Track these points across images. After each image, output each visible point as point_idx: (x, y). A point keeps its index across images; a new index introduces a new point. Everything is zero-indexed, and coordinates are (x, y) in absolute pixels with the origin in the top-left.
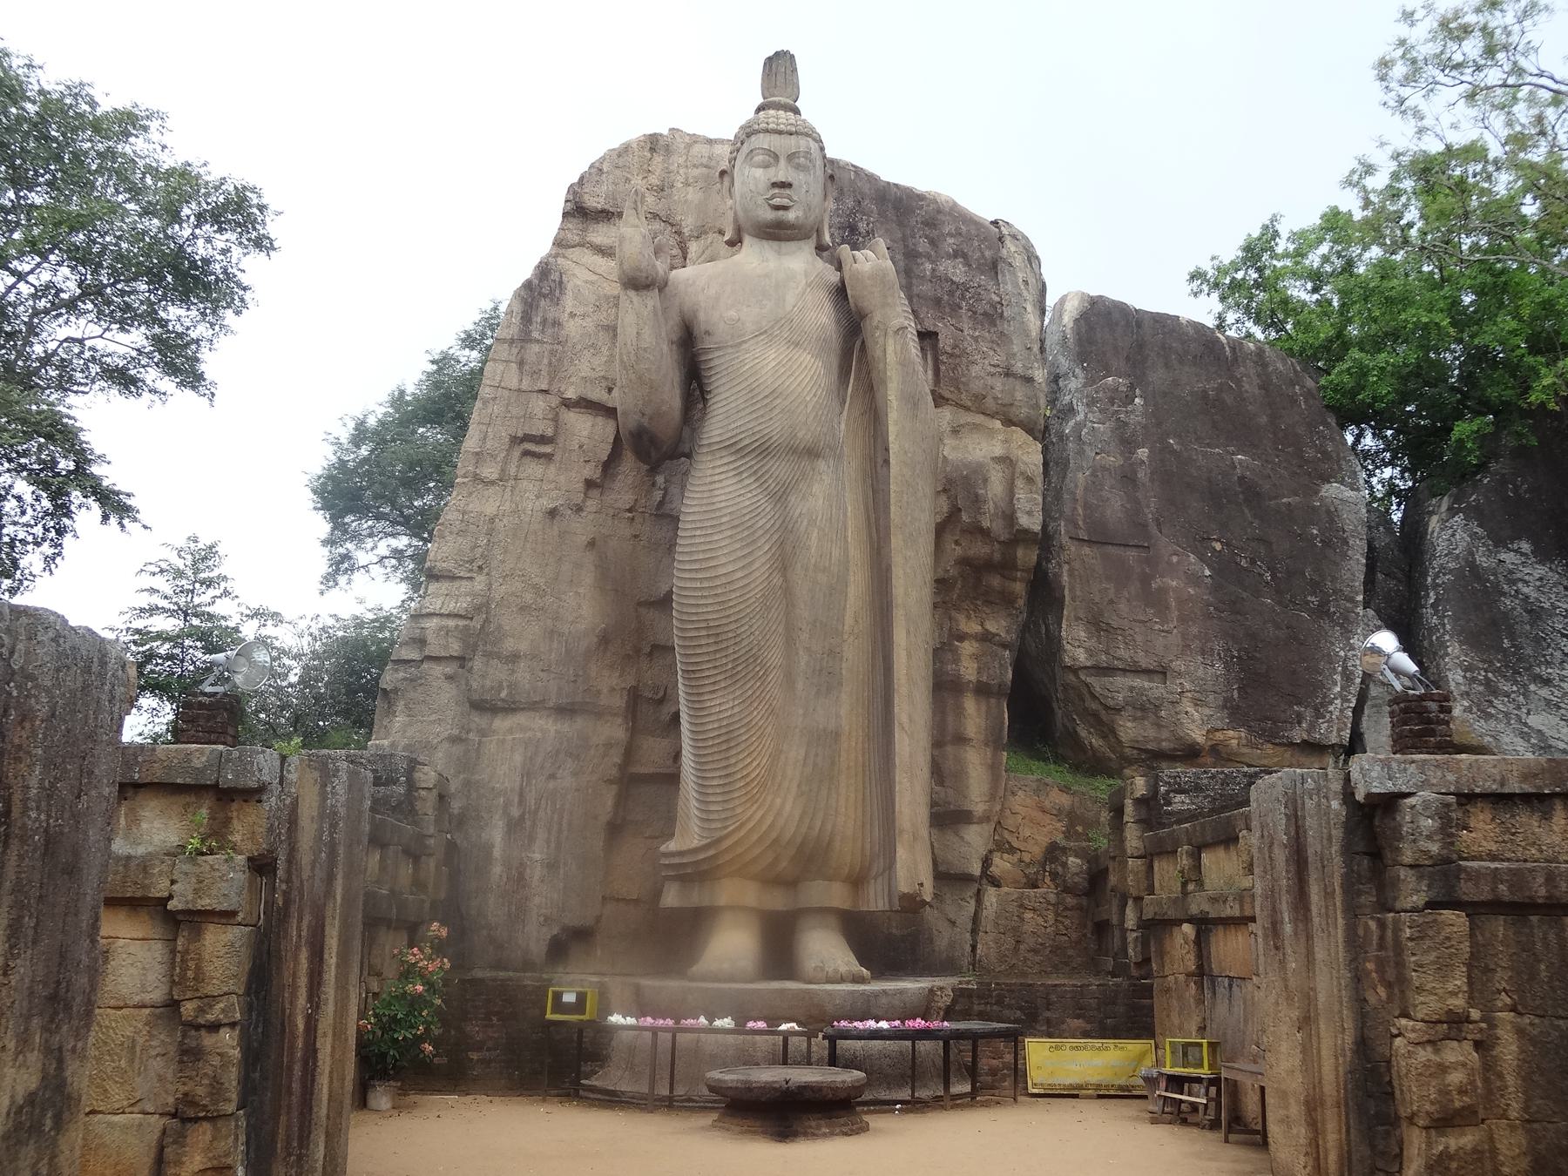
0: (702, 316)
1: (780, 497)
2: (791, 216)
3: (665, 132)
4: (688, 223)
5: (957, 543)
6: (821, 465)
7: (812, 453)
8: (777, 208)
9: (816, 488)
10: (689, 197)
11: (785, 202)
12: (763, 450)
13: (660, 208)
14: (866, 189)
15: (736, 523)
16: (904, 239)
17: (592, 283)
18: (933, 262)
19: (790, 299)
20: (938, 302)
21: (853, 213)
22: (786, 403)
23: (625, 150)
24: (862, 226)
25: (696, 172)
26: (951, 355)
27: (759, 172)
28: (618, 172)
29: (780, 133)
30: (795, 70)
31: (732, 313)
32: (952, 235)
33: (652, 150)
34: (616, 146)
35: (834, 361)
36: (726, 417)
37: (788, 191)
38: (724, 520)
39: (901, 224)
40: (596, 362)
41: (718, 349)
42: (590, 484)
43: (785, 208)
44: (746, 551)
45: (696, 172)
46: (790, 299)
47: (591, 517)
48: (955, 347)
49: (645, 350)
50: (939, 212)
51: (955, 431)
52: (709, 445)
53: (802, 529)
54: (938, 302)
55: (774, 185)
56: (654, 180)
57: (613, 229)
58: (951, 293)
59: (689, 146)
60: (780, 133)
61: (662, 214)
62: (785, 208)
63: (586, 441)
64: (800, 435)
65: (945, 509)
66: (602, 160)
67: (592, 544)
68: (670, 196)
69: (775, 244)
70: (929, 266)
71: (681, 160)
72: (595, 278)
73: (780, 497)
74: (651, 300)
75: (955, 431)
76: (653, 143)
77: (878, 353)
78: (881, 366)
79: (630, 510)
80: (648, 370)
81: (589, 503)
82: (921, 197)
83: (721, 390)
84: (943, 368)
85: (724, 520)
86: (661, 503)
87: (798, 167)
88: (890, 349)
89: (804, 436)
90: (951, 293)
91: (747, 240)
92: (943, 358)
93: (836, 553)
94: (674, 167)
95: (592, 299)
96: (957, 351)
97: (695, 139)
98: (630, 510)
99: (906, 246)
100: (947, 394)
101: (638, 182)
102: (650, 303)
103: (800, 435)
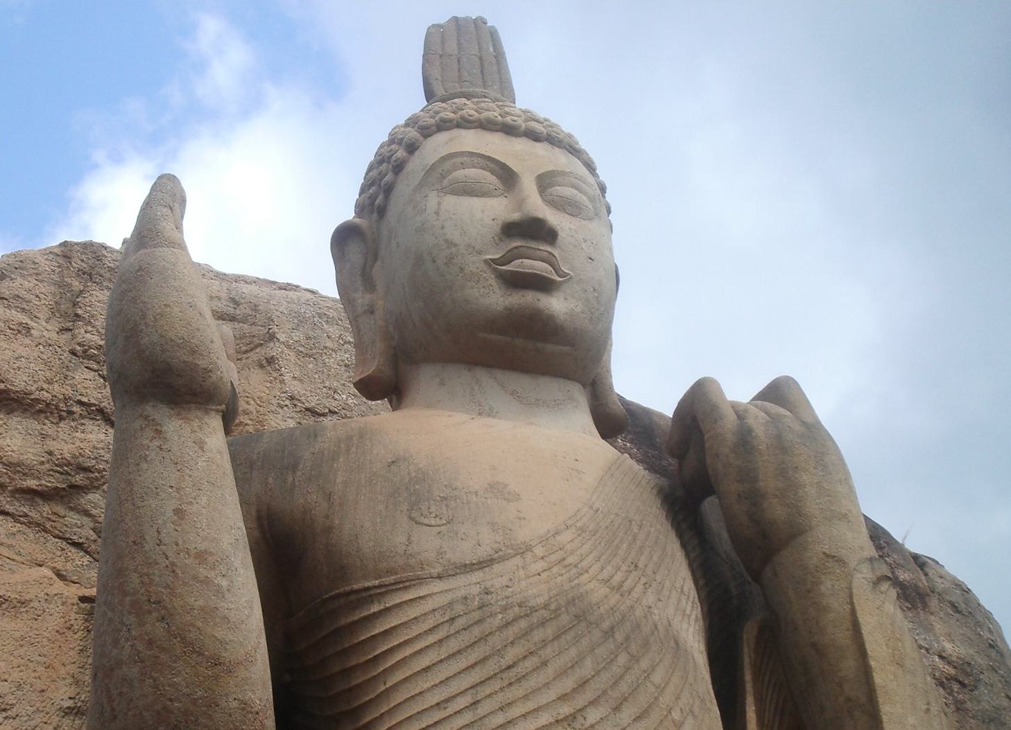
2: (557, 305)
43: (543, 285)
62: (543, 285)
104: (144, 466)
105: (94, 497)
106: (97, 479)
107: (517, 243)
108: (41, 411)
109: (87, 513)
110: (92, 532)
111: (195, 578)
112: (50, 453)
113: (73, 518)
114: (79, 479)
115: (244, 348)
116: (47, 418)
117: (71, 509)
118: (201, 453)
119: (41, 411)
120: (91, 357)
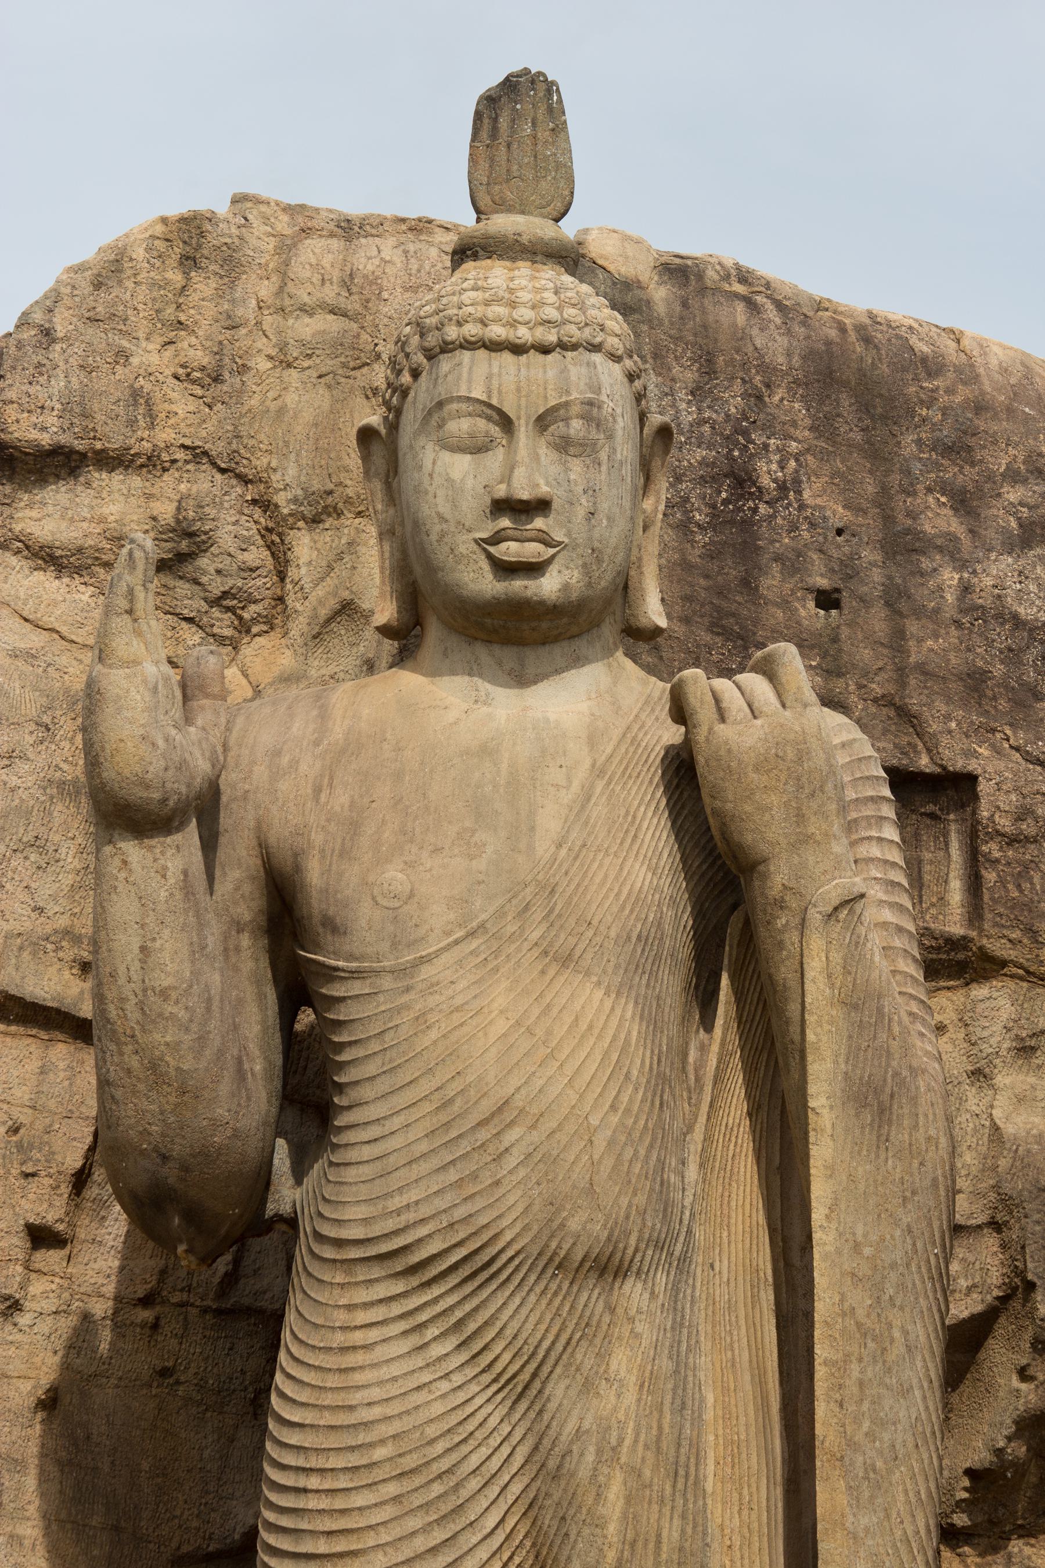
0: (314, 874)
1: (524, 1386)
2: (549, 586)
3: (222, 208)
4: (290, 480)
5: (1023, 1374)
6: (633, 1293)
7: (608, 1267)
8: (506, 569)
9: (622, 1362)
10: (291, 399)
11: (532, 551)
12: (478, 1267)
13: (210, 430)
14: (775, 345)
15: (410, 1462)
16: (883, 499)
17: (30, 656)
18: (961, 564)
19: (550, 822)
20: (975, 684)
21: (739, 431)
22: (535, 1137)
23: (111, 269)
24: (767, 472)
25: (306, 328)
26: (1013, 841)
27: (459, 465)
28: (91, 333)
29: (518, 349)
30: (560, 129)
31: (394, 876)
32: (1013, 477)
33: (189, 261)
34: (87, 248)
35: (672, 984)
36: (383, 1179)
37: (539, 523)
38: (380, 1453)
39: (878, 455)
40: (46, 888)
41: (356, 974)
42: (41, 1237)
43: (534, 569)
44: (439, 1535)
45: (306, 328)
46: (550, 822)
47: (44, 1326)
48: (1023, 814)
49: (164, 994)
50: (980, 407)
51: (1025, 1050)
52: (339, 1243)
53: (584, 1473)
54: (975, 684)
55: (503, 506)
56: (196, 353)
57: (85, 497)
58: (1013, 656)
59: (286, 248)
60: (518, 349)
61: (216, 448)
62: (534, 569)
63: (24, 1117)
64: (574, 1225)
65: (995, 1277)
66: (52, 301)
67: (50, 1403)
68: (240, 393)
69: (508, 655)
70: (950, 577)
71: (266, 290)
72: (36, 640)
73: (524, 1386)
74: (180, 852)
75: (1025, 1050)
76: (189, 241)
77: (785, 973)
78: (793, 1008)
79: (146, 1301)
80: (174, 1047)
81: (37, 1286)
82: (931, 366)
83: (367, 1092)
84: (990, 876)
85: (380, 1453)
86: (231, 1279)
87: (564, 446)
88: (814, 967)
89: (585, 1227)
90: (1013, 656)
91: (434, 632)
92: (992, 848)
93: (672, 1532)
94: (248, 311)
95: (30, 705)
96: (1028, 828)
97: (305, 223)
98: (146, 1301)
99: (888, 519)
100: (998, 948)
101: (149, 355)
102: (174, 865)
103: (574, 1225)
104: (114, 897)
105: (203, 562)
106: (204, 542)
107: (505, 522)
108: (142, 466)
109: (196, 582)
110: (203, 603)
111: (160, 1015)
112: (154, 519)
113: (183, 588)
114: (184, 545)
115: (352, 364)
116: (149, 472)
117: (181, 578)
118: (163, 881)
119: (142, 466)
120: (194, 382)
